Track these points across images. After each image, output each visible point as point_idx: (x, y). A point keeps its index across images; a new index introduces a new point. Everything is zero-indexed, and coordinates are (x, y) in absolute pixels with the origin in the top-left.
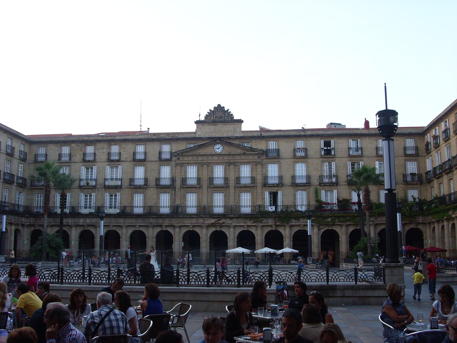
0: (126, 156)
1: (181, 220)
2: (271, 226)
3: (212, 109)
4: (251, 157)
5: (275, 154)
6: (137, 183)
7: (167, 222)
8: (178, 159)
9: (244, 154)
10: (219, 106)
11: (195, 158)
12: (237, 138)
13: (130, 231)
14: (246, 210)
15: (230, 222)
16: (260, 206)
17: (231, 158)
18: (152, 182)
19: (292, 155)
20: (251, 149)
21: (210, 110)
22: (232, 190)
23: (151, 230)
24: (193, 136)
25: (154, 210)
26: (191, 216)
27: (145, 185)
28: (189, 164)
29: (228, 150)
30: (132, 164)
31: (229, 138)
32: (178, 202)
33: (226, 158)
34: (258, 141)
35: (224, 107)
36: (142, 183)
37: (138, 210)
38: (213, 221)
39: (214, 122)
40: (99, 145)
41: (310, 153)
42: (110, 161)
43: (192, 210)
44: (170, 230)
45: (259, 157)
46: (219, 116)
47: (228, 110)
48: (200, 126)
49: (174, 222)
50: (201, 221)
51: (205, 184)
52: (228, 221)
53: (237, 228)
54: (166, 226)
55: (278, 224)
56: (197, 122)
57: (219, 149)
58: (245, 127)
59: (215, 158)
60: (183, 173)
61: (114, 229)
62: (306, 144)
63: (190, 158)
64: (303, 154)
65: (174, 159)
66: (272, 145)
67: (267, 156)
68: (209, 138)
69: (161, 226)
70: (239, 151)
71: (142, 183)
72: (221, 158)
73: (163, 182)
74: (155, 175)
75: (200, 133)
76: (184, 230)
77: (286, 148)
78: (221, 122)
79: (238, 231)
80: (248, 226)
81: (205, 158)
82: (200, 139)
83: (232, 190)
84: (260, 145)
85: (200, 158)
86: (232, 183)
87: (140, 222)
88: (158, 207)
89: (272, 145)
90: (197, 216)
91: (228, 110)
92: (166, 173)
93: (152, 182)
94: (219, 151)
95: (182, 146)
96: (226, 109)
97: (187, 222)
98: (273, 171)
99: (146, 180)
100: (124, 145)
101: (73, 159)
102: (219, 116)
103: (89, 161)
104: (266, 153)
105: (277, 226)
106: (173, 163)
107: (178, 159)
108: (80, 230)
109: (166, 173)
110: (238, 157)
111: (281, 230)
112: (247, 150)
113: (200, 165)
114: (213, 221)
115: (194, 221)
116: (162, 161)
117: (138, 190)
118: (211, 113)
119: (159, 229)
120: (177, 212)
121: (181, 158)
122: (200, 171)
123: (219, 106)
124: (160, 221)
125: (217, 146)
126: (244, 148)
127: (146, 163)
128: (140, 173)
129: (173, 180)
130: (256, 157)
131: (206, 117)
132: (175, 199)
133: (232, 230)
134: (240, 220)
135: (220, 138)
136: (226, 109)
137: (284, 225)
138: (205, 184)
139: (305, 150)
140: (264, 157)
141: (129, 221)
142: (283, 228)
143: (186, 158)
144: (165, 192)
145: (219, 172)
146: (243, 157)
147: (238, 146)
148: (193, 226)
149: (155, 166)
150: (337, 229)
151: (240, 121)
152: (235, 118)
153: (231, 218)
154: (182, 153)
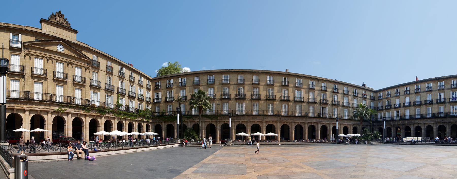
9: (80, 58)
10: (60, 12)
15: (70, 110)
21: (53, 14)
28: (36, 56)
29: (67, 52)
32: (27, 89)
35: (63, 15)
38: (56, 108)
43: (38, 97)
47: (67, 19)
52: (67, 109)
55: (98, 114)
57: (60, 49)
75: (46, 31)
91: (67, 19)
114: (56, 108)
118: (53, 16)
123: (60, 12)
125: (58, 47)
153: (70, 107)
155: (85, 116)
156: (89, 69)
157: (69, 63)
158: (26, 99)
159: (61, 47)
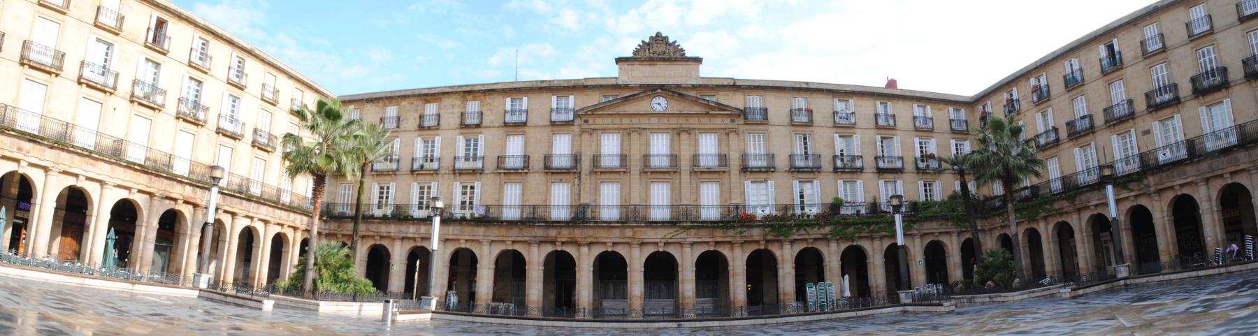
0: (492, 118)
1: (591, 232)
2: (757, 242)
3: (647, 40)
4: (719, 120)
5: (759, 117)
6: (510, 163)
7: (565, 233)
8: (586, 121)
9: (707, 114)
10: (658, 35)
11: (617, 120)
12: (694, 87)
13: (497, 249)
14: (710, 213)
15: (683, 235)
16: (737, 207)
17: (682, 120)
18: (537, 163)
19: (788, 120)
20: (721, 107)
22: (685, 177)
23: (535, 249)
24: (614, 82)
25: (541, 213)
26: (609, 225)
27: (524, 168)
28: (604, 130)
29: (677, 107)
30: (502, 130)
31: (679, 86)
32: (585, 200)
33: (673, 121)
34: (730, 94)
36: (518, 163)
37: (510, 214)
39: (651, 60)
40: (447, 101)
41: (817, 118)
42: (464, 126)
44: (571, 250)
45: (733, 121)
46: (659, 50)
48: (625, 66)
49: (578, 233)
50: (629, 233)
51: (636, 167)
53: (695, 247)
54: (563, 243)
55: (769, 238)
56: (619, 60)
57: (660, 104)
58: (707, 71)
59: (654, 120)
60: (594, 148)
61: (468, 246)
62: (808, 103)
63: (608, 120)
64: (804, 119)
65: (578, 122)
66: (755, 101)
67: (746, 118)
68: (641, 86)
69: (553, 242)
70: (696, 109)
71: (518, 163)
72: (665, 120)
73: (557, 163)
74: (544, 151)
76: (597, 251)
77: (778, 107)
78: (664, 60)
79: (699, 250)
80: (717, 243)
81: (635, 120)
82: (626, 87)
83: (685, 177)
84: (735, 101)
85: (626, 121)
86: (685, 165)
87: (514, 233)
88: (547, 207)
89: (755, 101)
90: (623, 223)
92: (562, 147)
93: (537, 163)
94: (658, 109)
95: (593, 99)
96: (671, 41)
97: (602, 234)
98: (755, 147)
99: (527, 159)
100: (488, 99)
101: (403, 126)
102: (659, 50)
103: (429, 128)
104: (743, 113)
105: (768, 241)
106: (576, 129)
107: (586, 121)
108: (409, 246)
109: (562, 147)
110: (695, 120)
111: (775, 249)
112: (712, 108)
113: (627, 133)
115: (616, 234)
116: (557, 126)
117: (513, 177)
118: (645, 46)
119: (549, 249)
120: (582, 218)
121: (591, 121)
122: (626, 143)
123: (658, 35)
124: (552, 233)
125: (657, 100)
126: (707, 105)
127: (526, 129)
128: (515, 147)
129: (576, 159)
130: (728, 121)
131: (636, 52)
132: (579, 195)
133: (687, 250)
134: (703, 232)
135: (662, 87)
136: (671, 41)
137: (779, 241)
138: (636, 167)
139: (810, 112)
140: (741, 121)
141: (494, 233)
142: (777, 245)
143: (599, 121)
144: (561, 181)
145: (660, 146)
146: (705, 120)
147: (696, 101)
148: (614, 243)
149: (543, 134)
150: (865, 244)
151: (698, 60)
152: (688, 55)
154: (594, 111)
155: (825, 239)
156: (736, 132)
157: (679, 132)
158: (582, 218)
159: (662, 101)
